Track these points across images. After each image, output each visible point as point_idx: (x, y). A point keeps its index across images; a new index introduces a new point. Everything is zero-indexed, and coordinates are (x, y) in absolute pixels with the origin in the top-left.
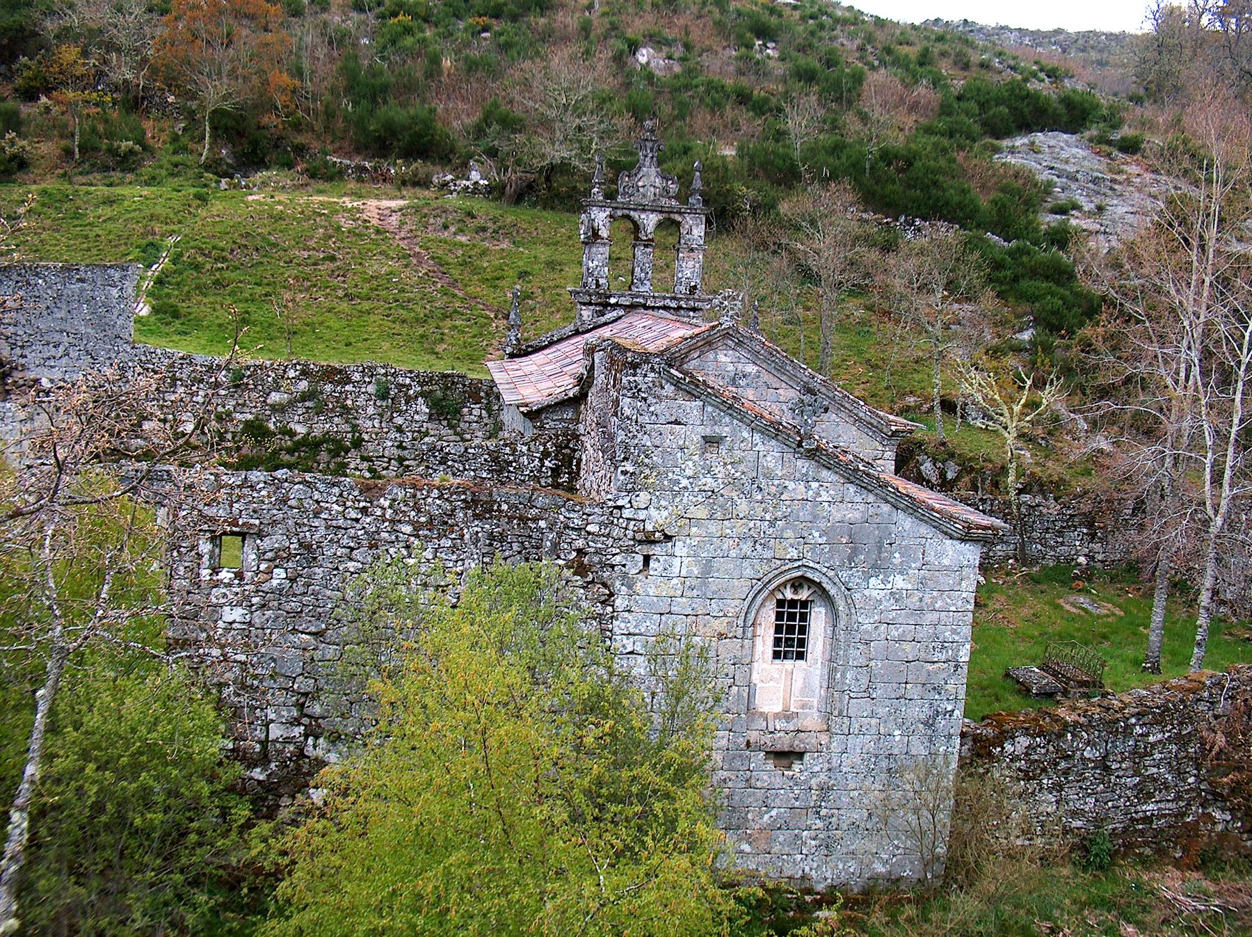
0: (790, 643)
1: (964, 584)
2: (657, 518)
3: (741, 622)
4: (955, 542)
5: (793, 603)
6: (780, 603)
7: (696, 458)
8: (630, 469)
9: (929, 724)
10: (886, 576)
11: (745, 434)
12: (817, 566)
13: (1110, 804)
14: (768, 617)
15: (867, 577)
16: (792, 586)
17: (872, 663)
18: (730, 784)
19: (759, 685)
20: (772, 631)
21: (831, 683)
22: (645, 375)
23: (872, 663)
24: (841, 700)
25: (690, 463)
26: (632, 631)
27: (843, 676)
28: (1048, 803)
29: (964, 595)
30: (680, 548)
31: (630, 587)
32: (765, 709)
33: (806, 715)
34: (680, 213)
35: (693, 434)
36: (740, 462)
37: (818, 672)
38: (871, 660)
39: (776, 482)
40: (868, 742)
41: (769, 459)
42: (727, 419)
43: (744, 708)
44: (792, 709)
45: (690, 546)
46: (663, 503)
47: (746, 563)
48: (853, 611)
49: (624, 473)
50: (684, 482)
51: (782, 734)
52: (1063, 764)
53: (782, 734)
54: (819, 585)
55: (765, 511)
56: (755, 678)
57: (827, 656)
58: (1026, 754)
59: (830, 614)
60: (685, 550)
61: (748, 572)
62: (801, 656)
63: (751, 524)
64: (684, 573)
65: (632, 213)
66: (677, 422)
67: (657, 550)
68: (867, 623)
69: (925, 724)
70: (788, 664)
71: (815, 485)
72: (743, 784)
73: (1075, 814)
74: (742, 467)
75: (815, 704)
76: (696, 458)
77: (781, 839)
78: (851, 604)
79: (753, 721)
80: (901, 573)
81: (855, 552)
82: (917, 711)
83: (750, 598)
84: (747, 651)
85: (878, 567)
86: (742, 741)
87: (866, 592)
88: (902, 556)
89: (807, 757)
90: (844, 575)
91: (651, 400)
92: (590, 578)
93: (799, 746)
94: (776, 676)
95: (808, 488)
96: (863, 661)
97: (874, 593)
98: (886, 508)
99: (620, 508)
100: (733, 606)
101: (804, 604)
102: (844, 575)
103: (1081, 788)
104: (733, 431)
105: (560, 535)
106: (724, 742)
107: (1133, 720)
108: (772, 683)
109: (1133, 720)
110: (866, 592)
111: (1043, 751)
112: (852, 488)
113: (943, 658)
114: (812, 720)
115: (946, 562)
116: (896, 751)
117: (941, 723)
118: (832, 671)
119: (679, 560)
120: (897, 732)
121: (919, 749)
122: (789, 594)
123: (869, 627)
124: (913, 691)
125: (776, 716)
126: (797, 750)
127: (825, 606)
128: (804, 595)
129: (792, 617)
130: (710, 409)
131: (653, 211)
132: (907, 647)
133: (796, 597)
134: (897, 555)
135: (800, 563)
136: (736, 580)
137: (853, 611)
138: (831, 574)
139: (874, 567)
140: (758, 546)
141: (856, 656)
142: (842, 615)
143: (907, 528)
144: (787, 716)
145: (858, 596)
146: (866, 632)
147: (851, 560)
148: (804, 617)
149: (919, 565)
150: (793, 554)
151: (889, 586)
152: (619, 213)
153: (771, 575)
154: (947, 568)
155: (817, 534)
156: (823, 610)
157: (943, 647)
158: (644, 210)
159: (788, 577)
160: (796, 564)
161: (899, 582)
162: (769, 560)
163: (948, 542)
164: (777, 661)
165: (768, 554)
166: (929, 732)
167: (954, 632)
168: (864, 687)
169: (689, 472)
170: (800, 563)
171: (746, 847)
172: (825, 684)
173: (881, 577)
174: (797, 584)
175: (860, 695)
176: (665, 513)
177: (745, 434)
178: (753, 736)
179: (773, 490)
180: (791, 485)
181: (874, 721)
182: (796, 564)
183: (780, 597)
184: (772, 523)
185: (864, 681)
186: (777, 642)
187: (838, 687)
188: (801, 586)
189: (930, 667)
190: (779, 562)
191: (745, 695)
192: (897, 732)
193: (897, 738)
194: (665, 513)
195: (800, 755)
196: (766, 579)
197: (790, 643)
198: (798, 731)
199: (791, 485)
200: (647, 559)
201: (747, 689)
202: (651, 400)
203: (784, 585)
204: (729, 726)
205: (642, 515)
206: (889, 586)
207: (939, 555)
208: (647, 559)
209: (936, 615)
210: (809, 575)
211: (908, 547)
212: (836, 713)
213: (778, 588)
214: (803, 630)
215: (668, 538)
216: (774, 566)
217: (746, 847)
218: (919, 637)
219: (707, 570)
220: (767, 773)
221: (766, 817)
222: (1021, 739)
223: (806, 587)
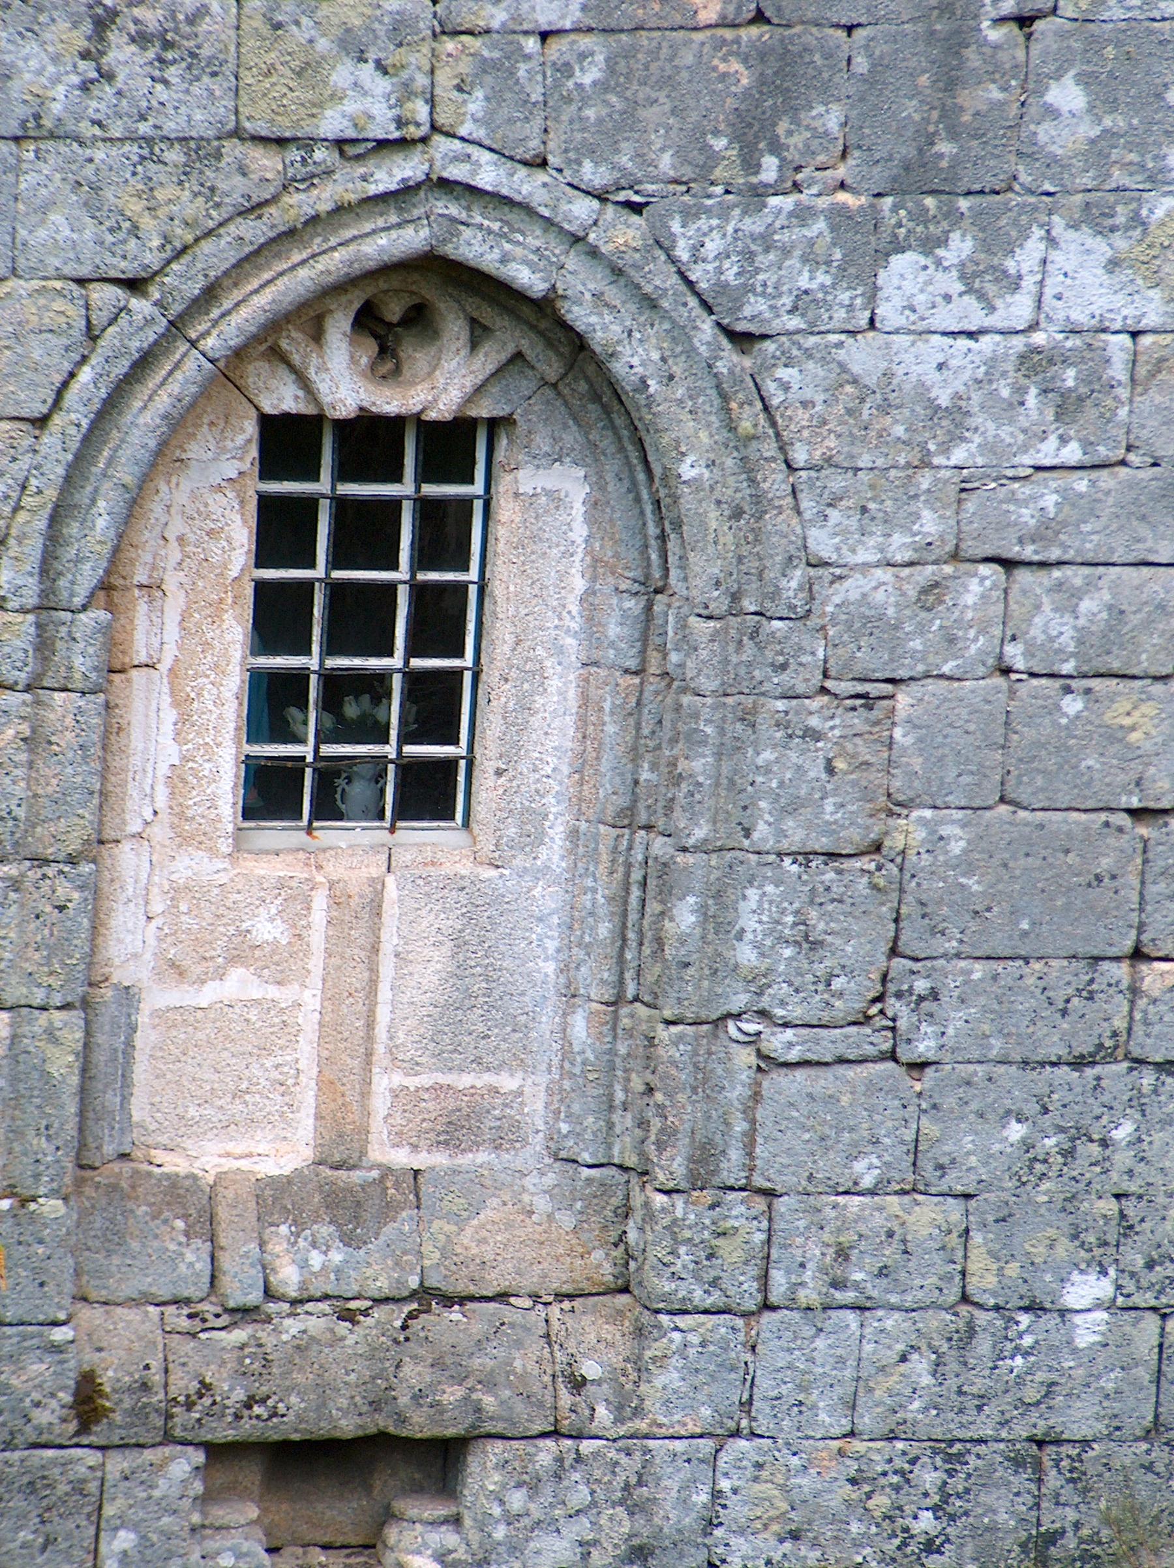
0: (361, 697)
5: (371, 442)
6: (286, 443)
10: (996, 241)
14: (210, 529)
15: (864, 251)
16: (367, 320)
17: (909, 832)
19: (158, 997)
20: (234, 630)
21: (637, 971)
23: (909, 832)
24: (705, 1084)
27: (718, 921)
32: (206, 1158)
33: (478, 1187)
37: (548, 898)
38: (896, 806)
40: (887, 1359)
43: (52, 1155)
44: (388, 1152)
48: (775, 481)
51: (314, 1322)
53: (314, 1322)
54: (542, 314)
56: (132, 945)
57: (608, 791)
59: (620, 511)
62: (430, 793)
68: (865, 563)
70: (352, 848)
75: (536, 1107)
78: (756, 435)
79: (114, 1239)
80: (1095, 218)
81: (783, 83)
83: (76, 413)
84: (65, 772)
87: (861, 356)
89: (484, 1471)
90: (708, 243)
93: (426, 1401)
94: (267, 929)
96: (840, 817)
97: (918, 362)
101: (451, 445)
108: (240, 983)
110: (861, 356)
114: (515, 1221)
116: (1079, 1418)
118: (643, 890)
120: (1086, 1290)
122: (343, 383)
123: (879, 589)
125: (276, 1200)
126: (420, 1425)
127: (591, 455)
128: (442, 382)
133: (389, 402)
134: (1067, 95)
135: (405, 168)
137: (775, 481)
138: (623, 234)
139: (915, 178)
140: (121, 53)
141: (799, 781)
142: (705, 517)
144: (341, 1194)
145: (794, 382)
146: (867, 622)
147: (753, 133)
148: (446, 535)
150: (363, 100)
151: (1019, 309)
153: (216, 255)
156: (572, 485)
159: (334, 260)
162: (200, 151)
164: (277, 835)
165: (192, 107)
168: (853, 992)
170: (405, 168)
172: (595, 978)
173: (960, 247)
174: (397, 307)
175: (829, 1043)
178: (121, 1343)
181: (926, 1218)
183: (283, 398)
185: (857, 949)
186: (273, 703)
187: (687, 994)
188: (419, 319)
190: (267, 163)
191: (62, 1064)
192: (1086, 1290)
193: (1088, 1330)
195: (438, 1461)
196: (184, 282)
197: (361, 697)
198: (428, 1297)
201: (70, 1026)
203: (309, 316)
206: (1019, 309)
210: (476, 247)
212: (673, 1165)
213: (268, 343)
214: (443, 620)
216: (234, 188)
223: (455, 329)
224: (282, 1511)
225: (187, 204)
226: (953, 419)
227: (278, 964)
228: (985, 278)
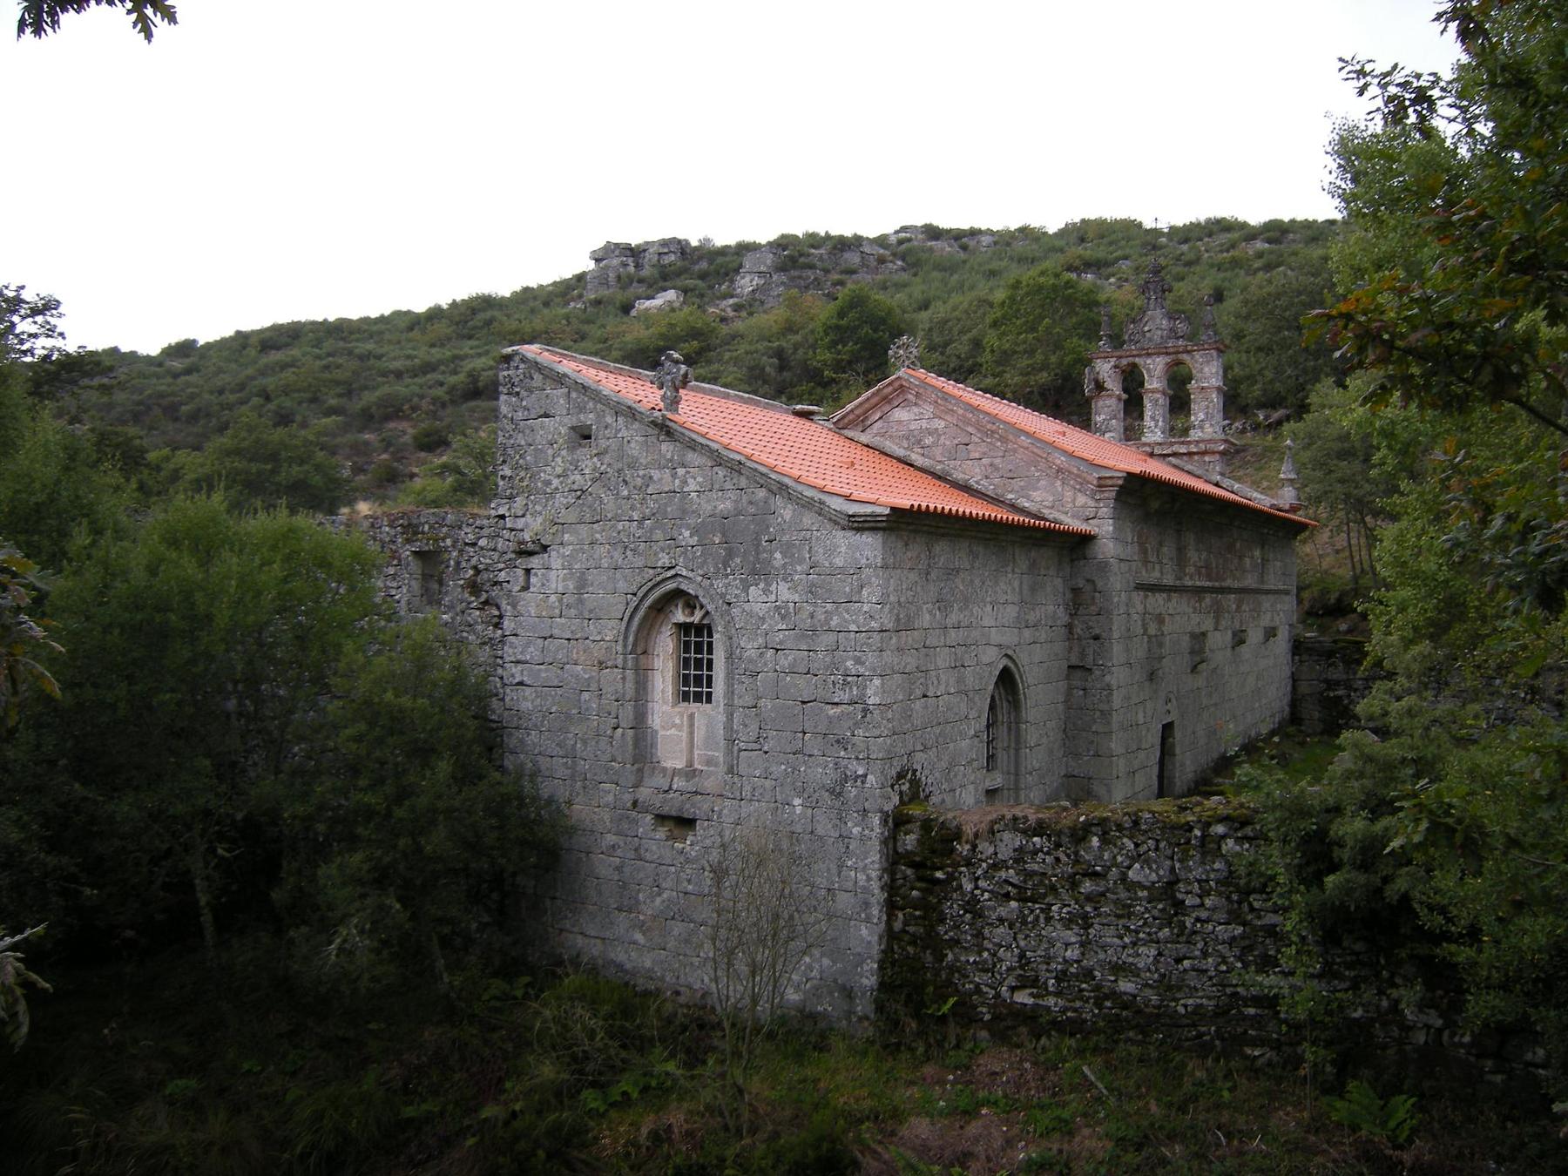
1: (864, 592)
2: (532, 527)
3: (620, 648)
4: (849, 534)
7: (564, 453)
8: (508, 472)
9: (836, 793)
11: (609, 420)
12: (690, 575)
13: (1186, 963)
14: (665, 646)
17: (762, 702)
18: (619, 852)
19: (661, 733)
22: (517, 368)
23: (762, 702)
25: (559, 460)
26: (519, 657)
28: (1065, 944)
29: (866, 608)
30: (555, 559)
31: (514, 607)
34: (1188, 352)
35: (559, 426)
36: (605, 451)
39: (641, 473)
41: (633, 445)
42: (591, 405)
45: (564, 556)
46: (538, 508)
47: (618, 574)
49: (503, 477)
50: (556, 482)
52: (1087, 886)
55: (633, 508)
58: (1016, 861)
60: (560, 561)
61: (622, 586)
63: (620, 526)
64: (560, 590)
65: (1137, 360)
66: (546, 416)
67: (535, 562)
69: (831, 791)
71: (681, 471)
72: (632, 855)
73: (1118, 969)
74: (607, 459)
76: (564, 453)
77: (676, 932)
80: (784, 579)
81: (730, 554)
82: (820, 773)
83: (626, 618)
85: (759, 572)
86: (627, 798)
87: (747, 607)
88: (784, 555)
91: (523, 393)
92: (484, 596)
94: (678, 722)
95: (674, 476)
96: (748, 700)
98: (761, 493)
99: (503, 517)
100: (611, 630)
102: (719, 584)
103: (1127, 928)
104: (600, 416)
105: (461, 551)
106: (610, 798)
107: (1220, 829)
108: (673, 731)
109: (1220, 829)
110: (747, 607)
111: (1049, 859)
112: (721, 472)
113: (846, 697)
115: (839, 562)
117: (851, 791)
119: (553, 575)
120: (797, 801)
121: (825, 827)
124: (813, 745)
125: (675, 772)
129: (699, 650)
130: (574, 395)
131: (1159, 354)
132: (801, 681)
133: (689, 620)
134: (778, 555)
135: (672, 572)
136: (613, 597)
139: (754, 572)
140: (629, 553)
143: (787, 518)
144: (690, 773)
146: (751, 661)
149: (805, 567)
150: (664, 560)
152: (1124, 362)
153: (645, 589)
154: (842, 570)
155: (687, 534)
157: (845, 683)
158: (1149, 355)
160: (670, 573)
161: (783, 592)
163: (841, 533)
166: (838, 804)
167: (858, 661)
169: (559, 470)
170: (672, 572)
171: (639, 937)
173: (762, 585)
176: (540, 520)
177: (609, 420)
178: (644, 793)
179: (639, 481)
180: (656, 474)
181: (768, 784)
182: (670, 573)
184: (641, 522)
189: (832, 711)
192: (797, 801)
194: (540, 520)
196: (640, 594)
199: (656, 474)
200: (528, 571)
202: (523, 393)
204: (615, 778)
205: (520, 523)
206: (773, 598)
207: (831, 551)
208: (528, 571)
209: (832, 637)
210: (683, 587)
211: (790, 545)
215: (545, 548)
216: (647, 577)
217: (639, 937)
218: (814, 667)
219: (582, 584)
220: (656, 840)
221: (658, 900)
222: (1007, 836)
224: (676, 832)
225: (639, 579)
226: (763, 619)
227: (679, 728)
228: (766, 591)
